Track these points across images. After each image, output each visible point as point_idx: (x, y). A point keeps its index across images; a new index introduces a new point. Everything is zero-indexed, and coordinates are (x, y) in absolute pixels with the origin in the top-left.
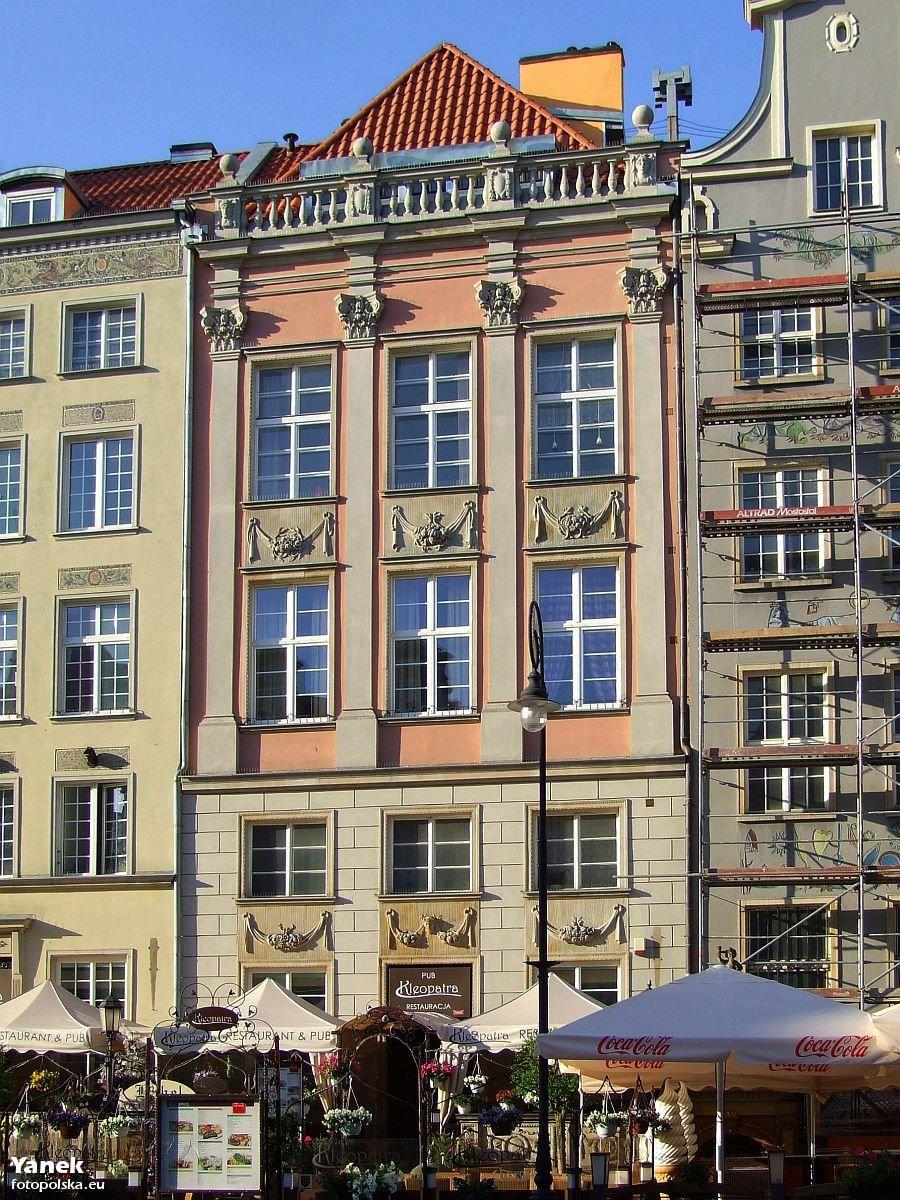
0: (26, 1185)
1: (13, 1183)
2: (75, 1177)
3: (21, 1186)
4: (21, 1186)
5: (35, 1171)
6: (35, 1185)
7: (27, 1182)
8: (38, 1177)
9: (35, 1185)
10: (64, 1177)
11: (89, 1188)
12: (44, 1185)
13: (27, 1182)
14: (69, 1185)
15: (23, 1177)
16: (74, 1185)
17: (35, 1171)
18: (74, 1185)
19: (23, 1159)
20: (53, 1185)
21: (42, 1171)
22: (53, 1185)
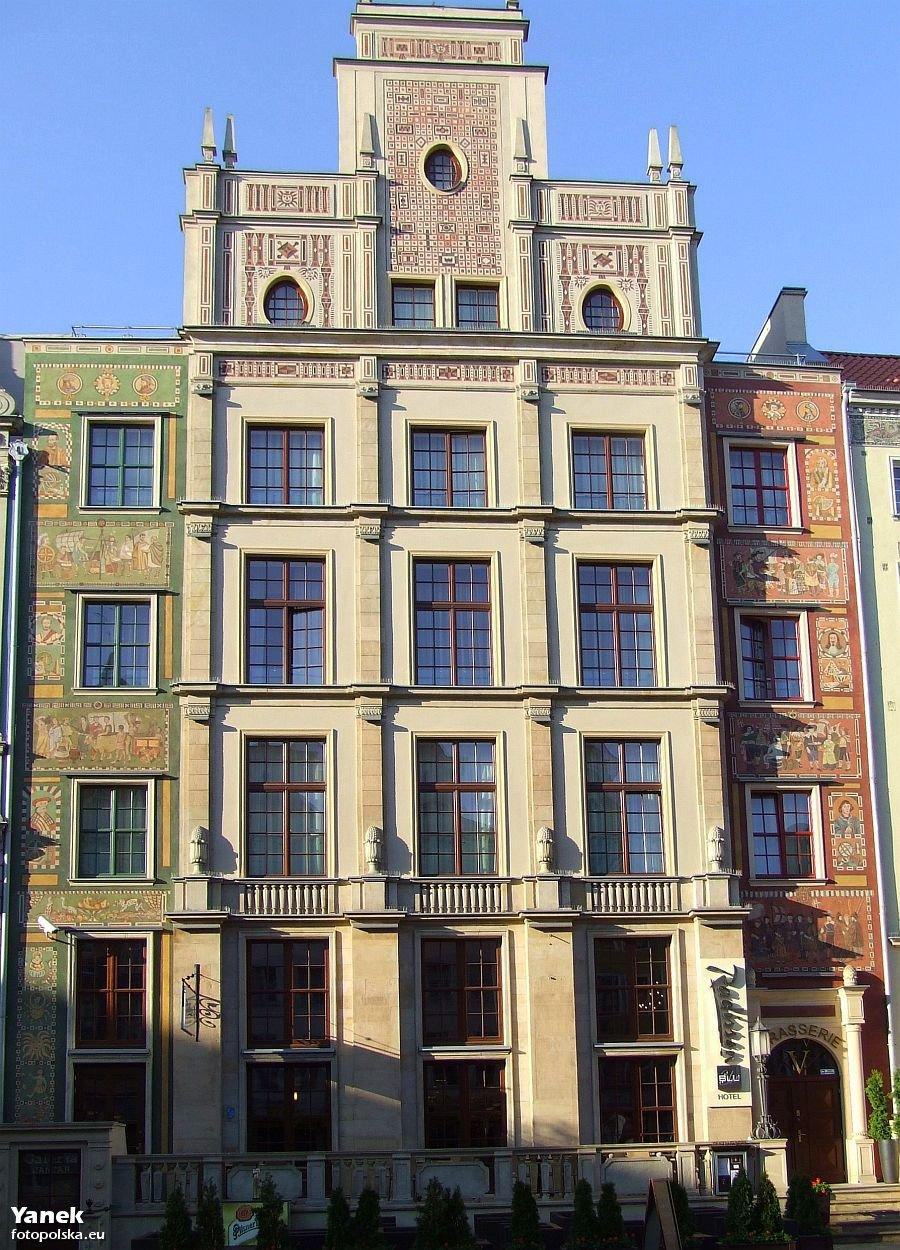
0: (26, 1235)
1: (13, 1233)
2: (75, 1227)
3: (21, 1235)
4: (21, 1235)
5: (35, 1221)
6: (35, 1235)
7: (28, 1232)
8: (33, 1227)
9: (35, 1235)
10: (64, 1227)
11: (89, 1239)
12: (44, 1235)
13: (28, 1232)
14: (70, 1235)
15: (23, 1227)
16: (74, 1235)
17: (35, 1221)
18: (74, 1235)
19: (24, 1209)
20: (53, 1236)
21: (43, 1221)
22: (53, 1236)
